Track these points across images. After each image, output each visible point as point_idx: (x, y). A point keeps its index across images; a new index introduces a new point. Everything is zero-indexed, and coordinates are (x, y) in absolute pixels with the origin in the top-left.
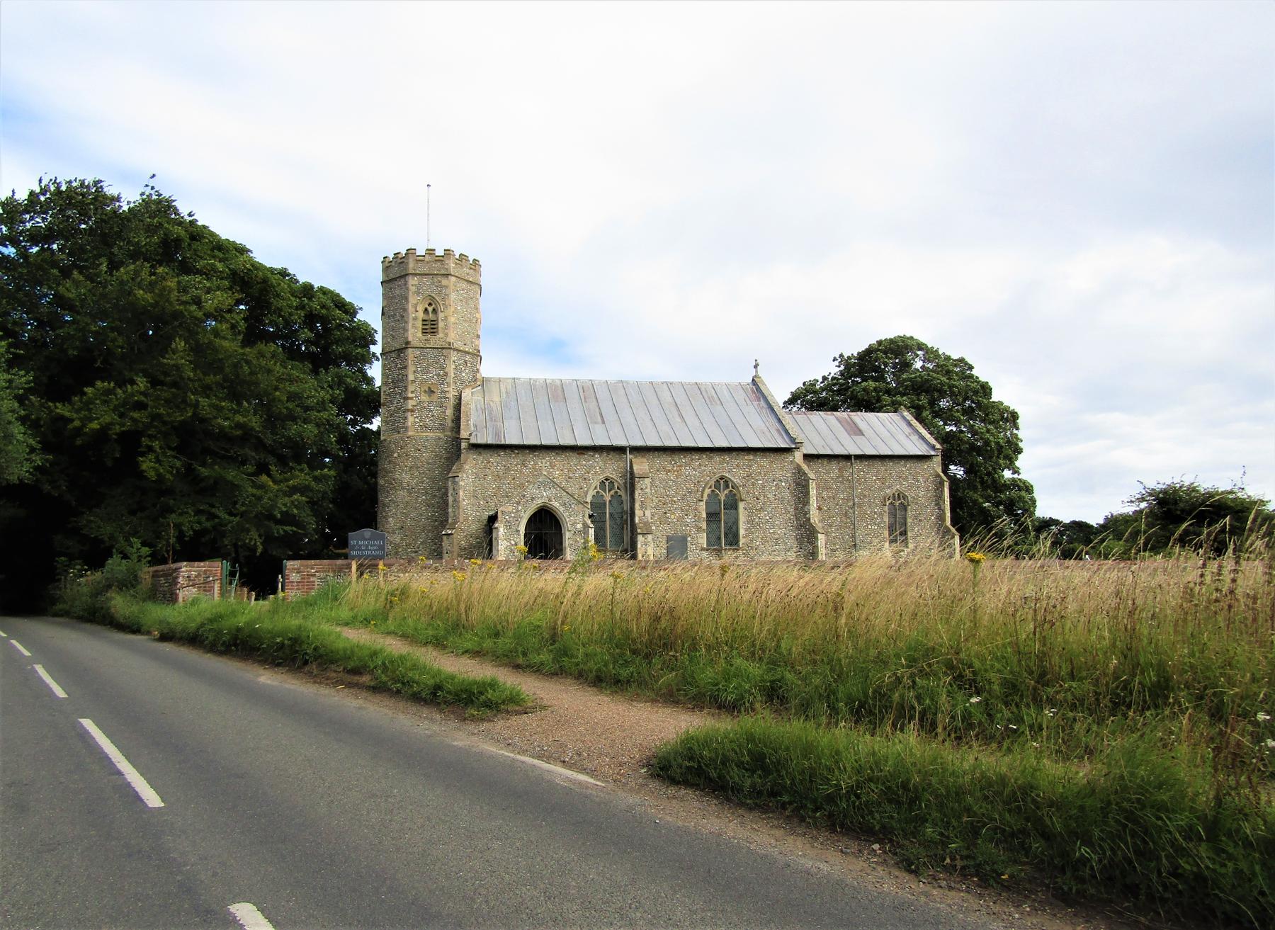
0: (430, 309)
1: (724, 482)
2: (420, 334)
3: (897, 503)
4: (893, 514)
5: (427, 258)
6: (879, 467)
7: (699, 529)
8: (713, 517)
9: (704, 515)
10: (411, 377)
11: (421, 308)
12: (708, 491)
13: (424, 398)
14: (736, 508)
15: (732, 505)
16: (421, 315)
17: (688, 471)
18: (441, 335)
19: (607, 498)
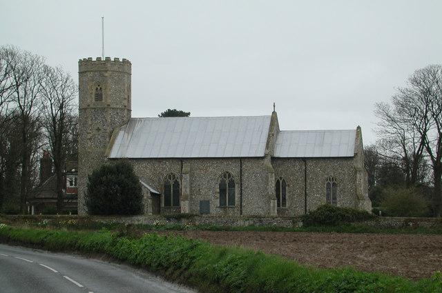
0: (99, 88)
1: (227, 175)
2: (94, 101)
3: (331, 183)
4: (328, 188)
5: (97, 63)
6: (322, 163)
7: (214, 197)
8: (222, 191)
9: (218, 190)
10: (90, 123)
11: (94, 89)
12: (220, 179)
13: (95, 132)
14: (234, 186)
15: (232, 184)
16: (94, 91)
17: (211, 169)
18: (103, 101)
19: (172, 182)
